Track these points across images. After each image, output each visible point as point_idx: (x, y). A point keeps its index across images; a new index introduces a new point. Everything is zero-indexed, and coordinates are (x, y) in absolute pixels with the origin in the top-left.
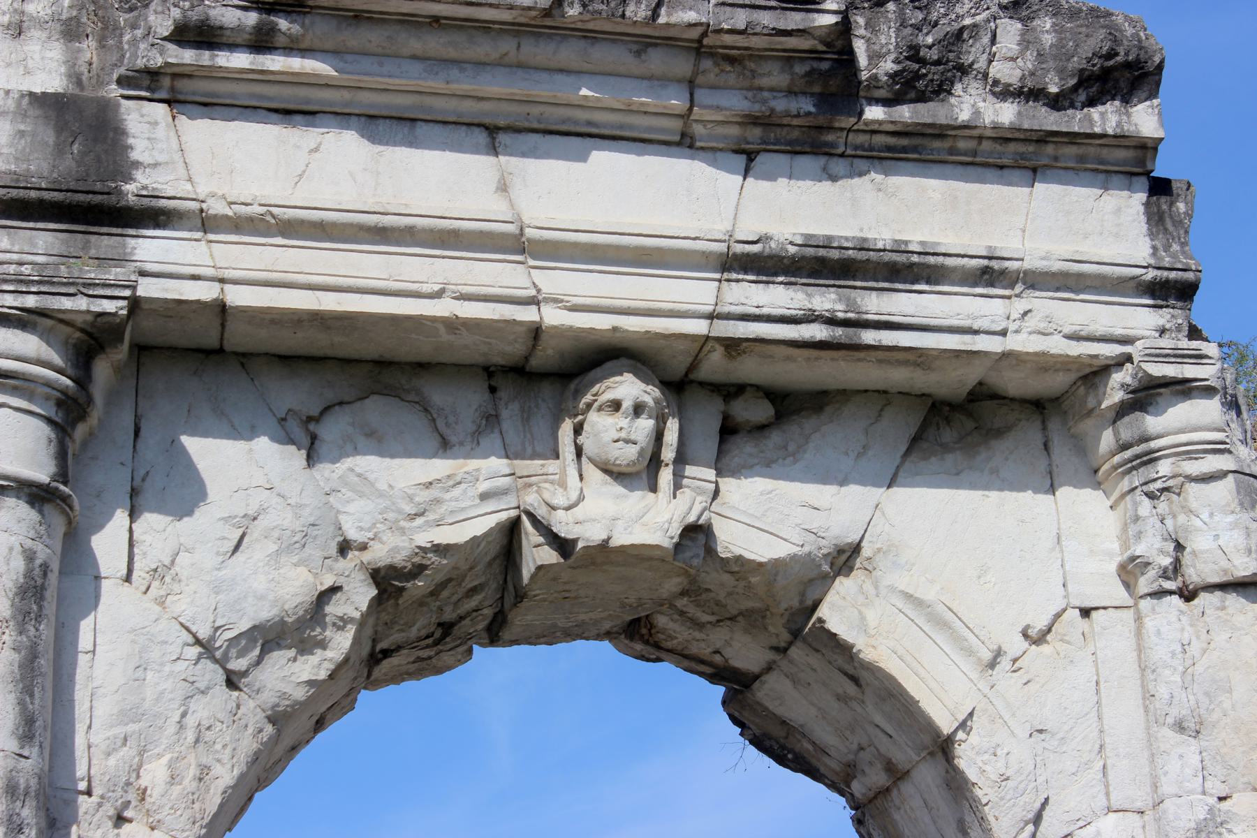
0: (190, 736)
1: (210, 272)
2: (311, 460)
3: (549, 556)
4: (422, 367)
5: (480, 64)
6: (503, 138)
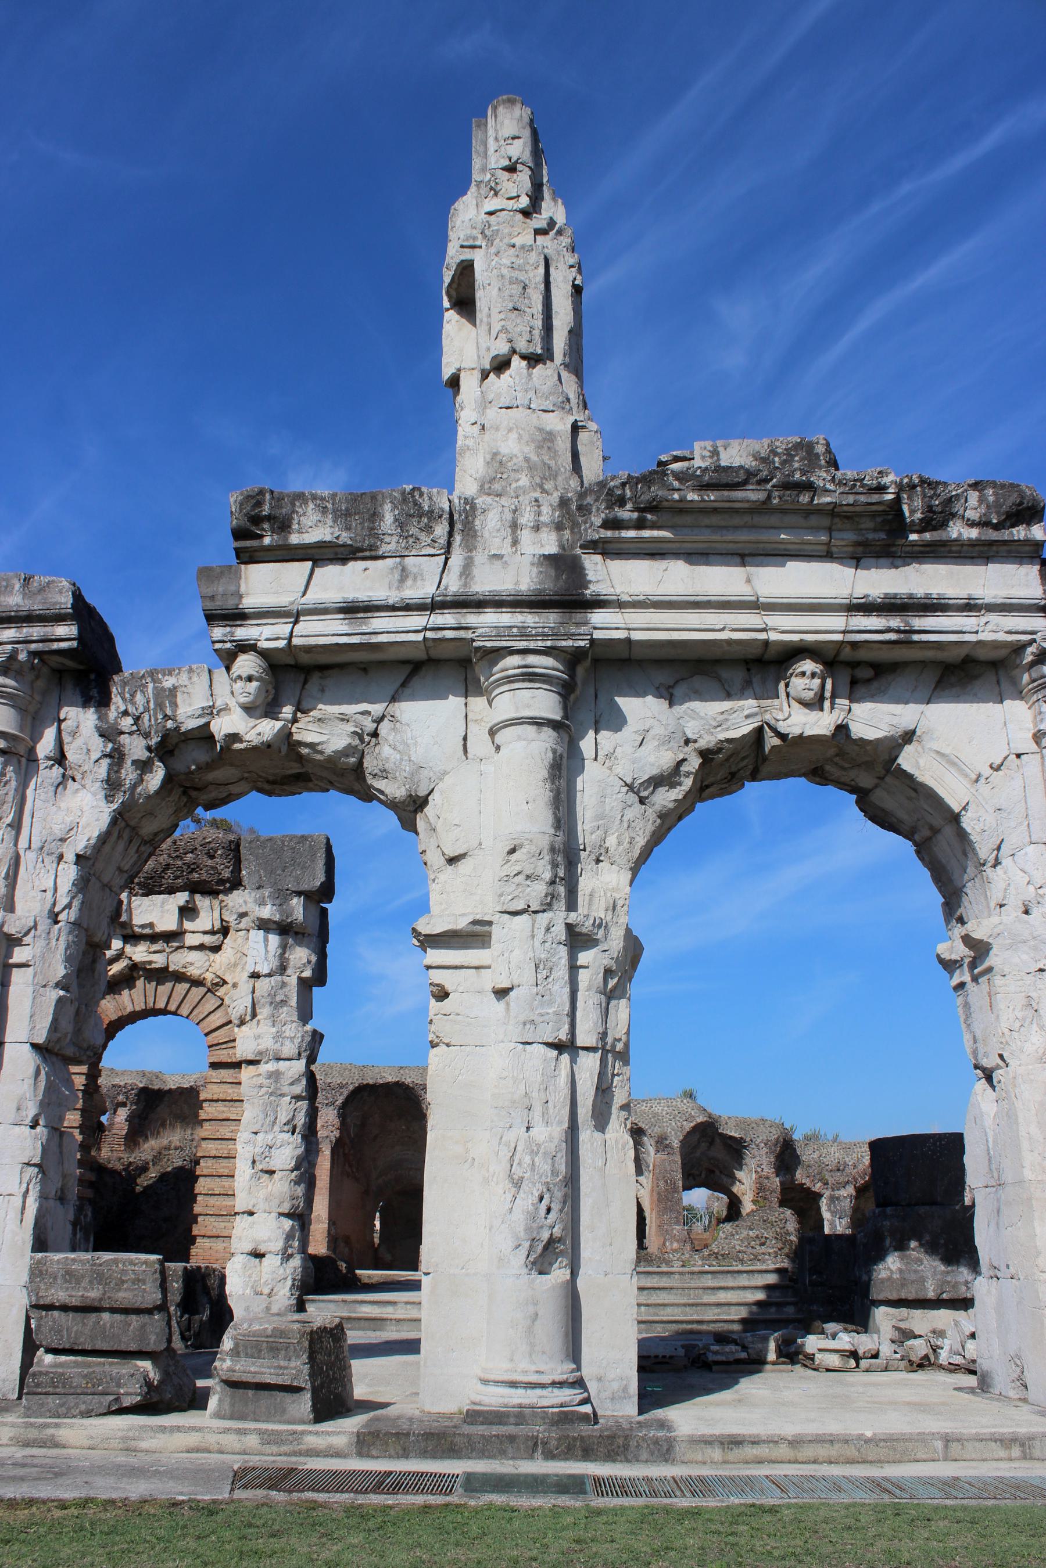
0: (626, 825)
1: (623, 626)
2: (671, 705)
3: (776, 741)
4: (718, 662)
5: (736, 528)
6: (747, 559)
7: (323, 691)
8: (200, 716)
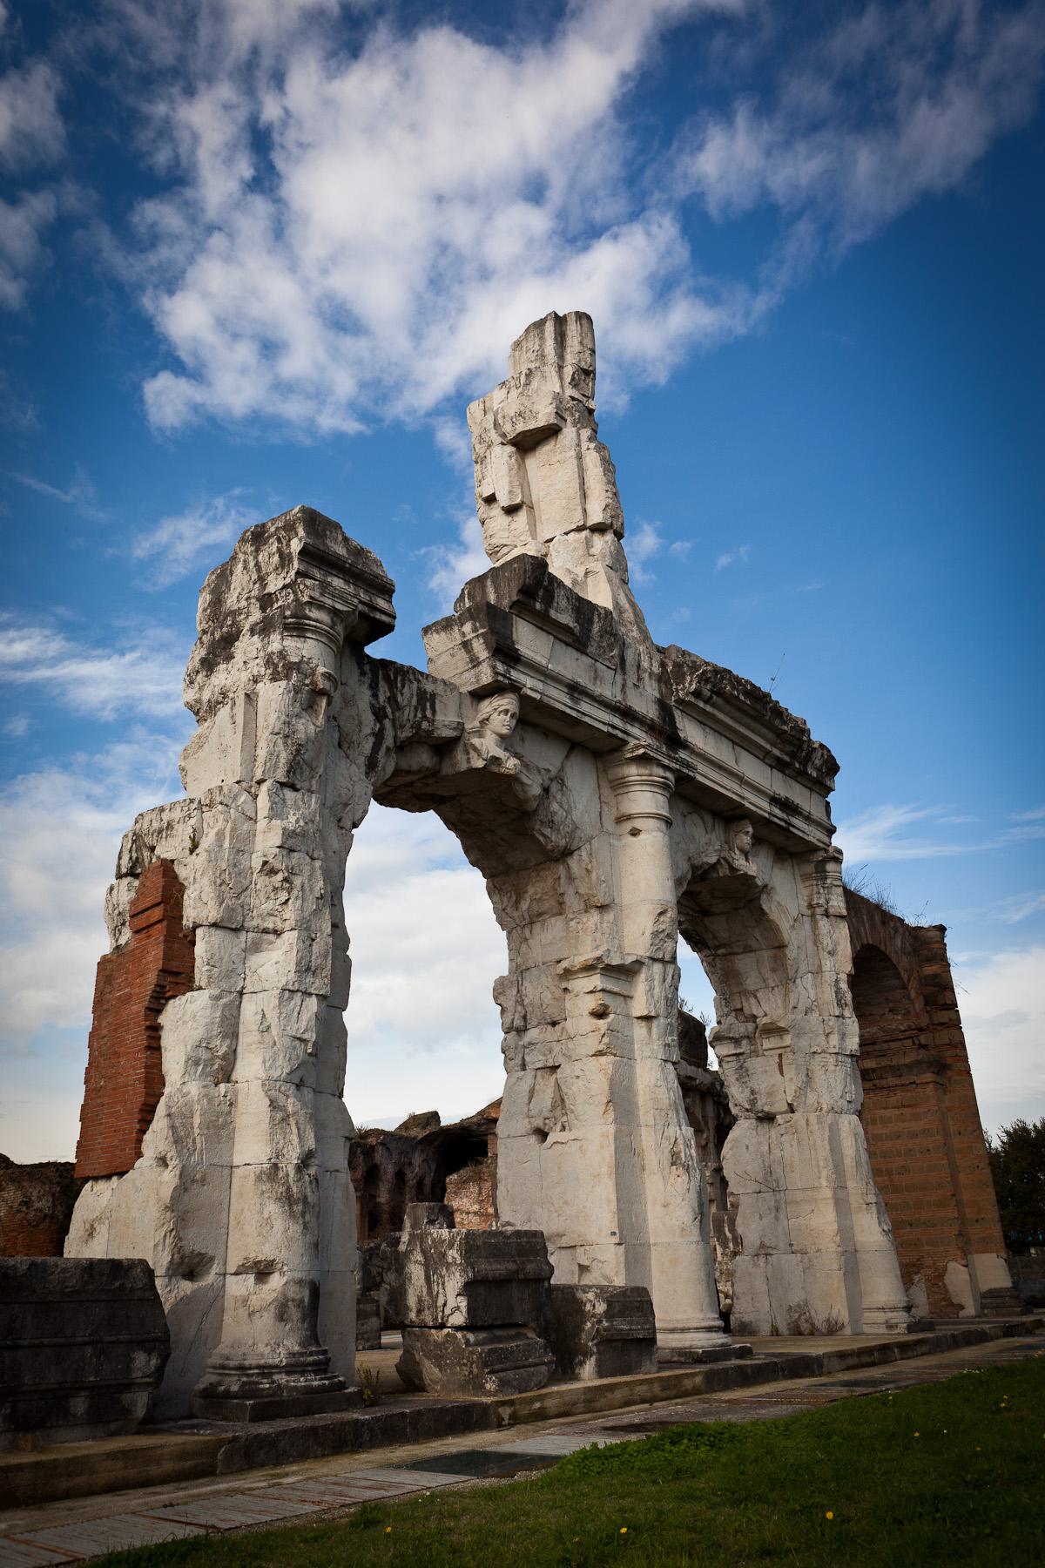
7: (523, 740)
8: (454, 729)
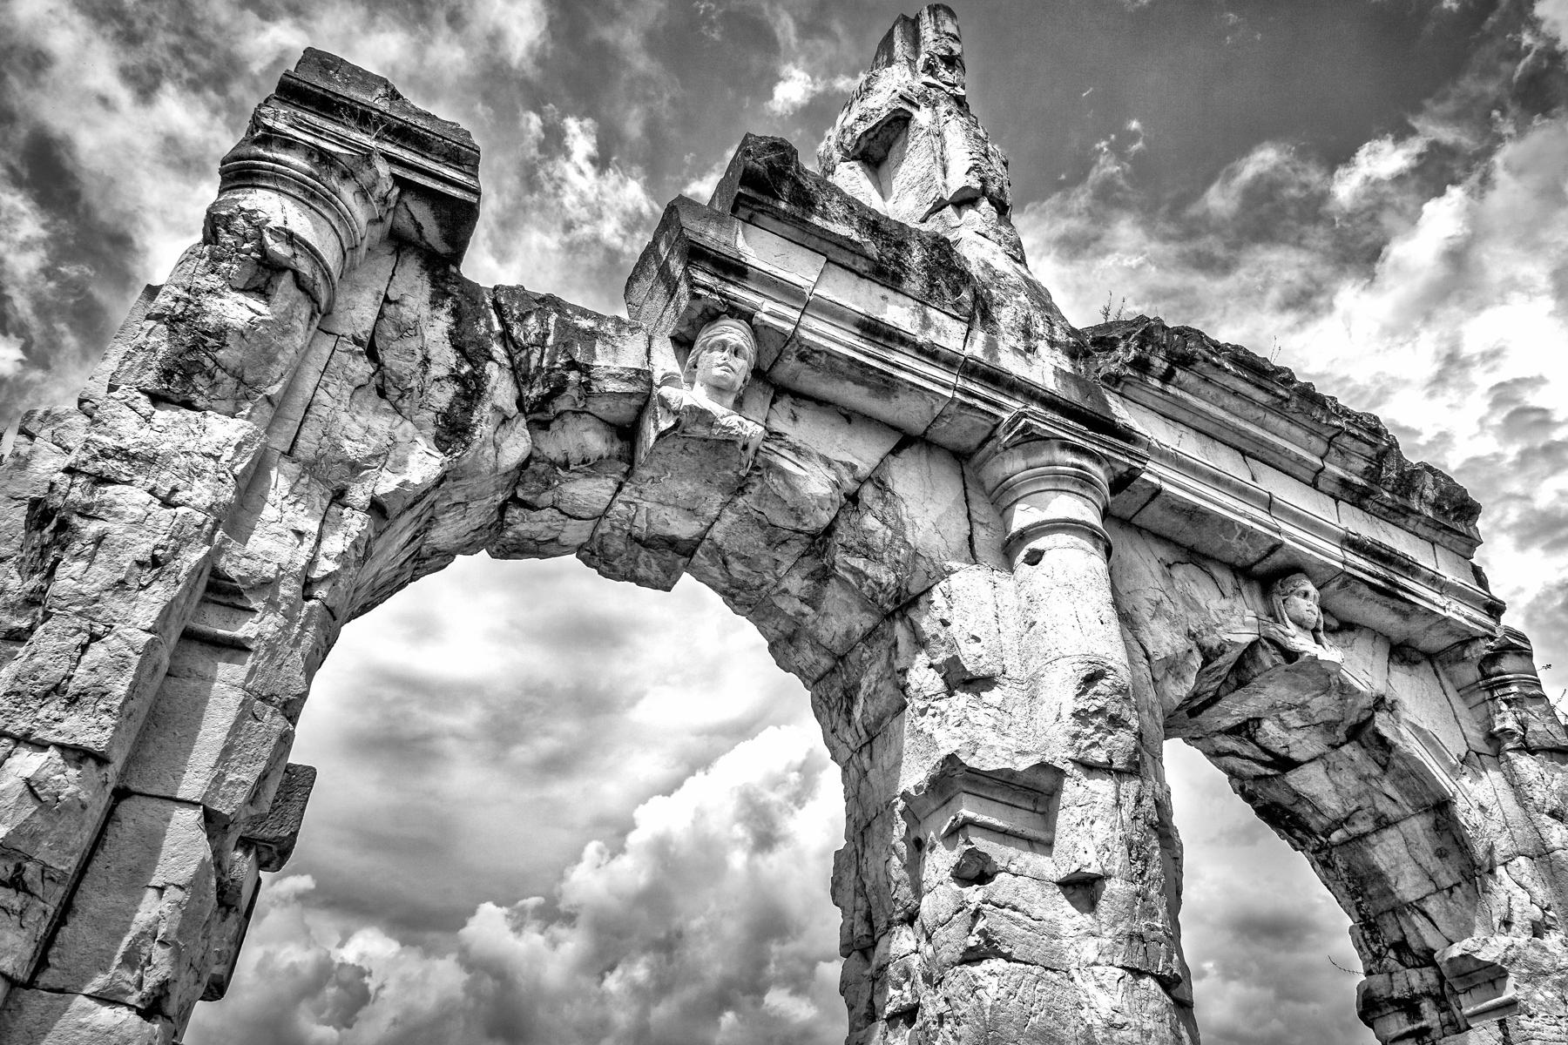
8: (629, 380)
